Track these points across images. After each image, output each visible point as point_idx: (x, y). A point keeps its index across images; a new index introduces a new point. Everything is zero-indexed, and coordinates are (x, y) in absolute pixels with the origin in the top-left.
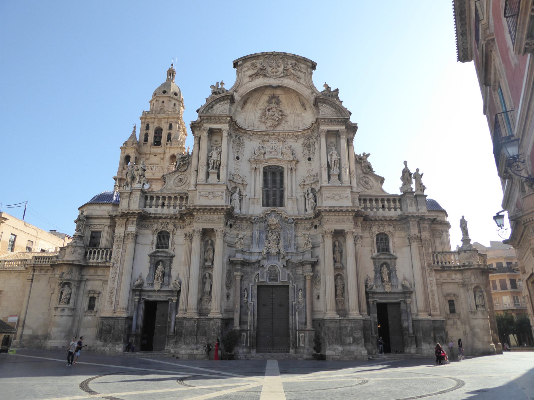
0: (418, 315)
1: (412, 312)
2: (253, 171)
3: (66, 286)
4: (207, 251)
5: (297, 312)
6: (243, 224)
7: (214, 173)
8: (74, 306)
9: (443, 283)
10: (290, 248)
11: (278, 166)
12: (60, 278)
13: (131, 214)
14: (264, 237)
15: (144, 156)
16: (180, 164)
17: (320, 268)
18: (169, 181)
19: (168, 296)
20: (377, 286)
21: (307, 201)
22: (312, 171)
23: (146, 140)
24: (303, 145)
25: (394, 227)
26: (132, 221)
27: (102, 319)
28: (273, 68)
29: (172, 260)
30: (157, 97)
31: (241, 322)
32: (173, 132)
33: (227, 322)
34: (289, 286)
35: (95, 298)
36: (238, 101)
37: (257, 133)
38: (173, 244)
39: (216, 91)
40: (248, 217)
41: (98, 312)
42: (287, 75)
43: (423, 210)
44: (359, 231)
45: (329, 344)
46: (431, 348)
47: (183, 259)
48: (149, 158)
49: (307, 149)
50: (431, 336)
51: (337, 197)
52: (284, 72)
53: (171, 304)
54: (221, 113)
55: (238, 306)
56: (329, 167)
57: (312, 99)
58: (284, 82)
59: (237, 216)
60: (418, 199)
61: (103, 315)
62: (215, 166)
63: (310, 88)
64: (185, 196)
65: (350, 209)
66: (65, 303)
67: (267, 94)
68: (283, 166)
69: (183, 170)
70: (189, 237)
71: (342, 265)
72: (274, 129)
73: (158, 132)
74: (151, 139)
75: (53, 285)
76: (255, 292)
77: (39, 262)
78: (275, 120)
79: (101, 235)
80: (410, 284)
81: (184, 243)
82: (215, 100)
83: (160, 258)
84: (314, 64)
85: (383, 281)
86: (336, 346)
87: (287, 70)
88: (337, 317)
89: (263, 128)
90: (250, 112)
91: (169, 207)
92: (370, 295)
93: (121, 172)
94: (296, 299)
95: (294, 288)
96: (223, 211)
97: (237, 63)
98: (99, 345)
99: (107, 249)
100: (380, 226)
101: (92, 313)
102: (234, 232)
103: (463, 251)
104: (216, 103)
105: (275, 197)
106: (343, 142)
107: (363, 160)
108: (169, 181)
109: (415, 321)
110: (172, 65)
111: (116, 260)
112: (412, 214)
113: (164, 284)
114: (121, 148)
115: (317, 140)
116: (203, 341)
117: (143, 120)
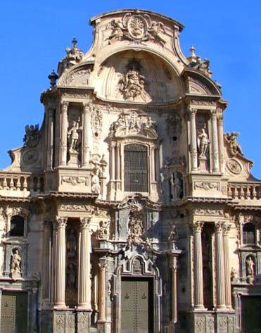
28: (136, 29)
44: (227, 223)
57: (180, 68)
81: (42, 229)
83: (15, 246)
85: (247, 274)
89: (120, 99)
91: (22, 189)
97: (95, 21)
115: (185, 118)
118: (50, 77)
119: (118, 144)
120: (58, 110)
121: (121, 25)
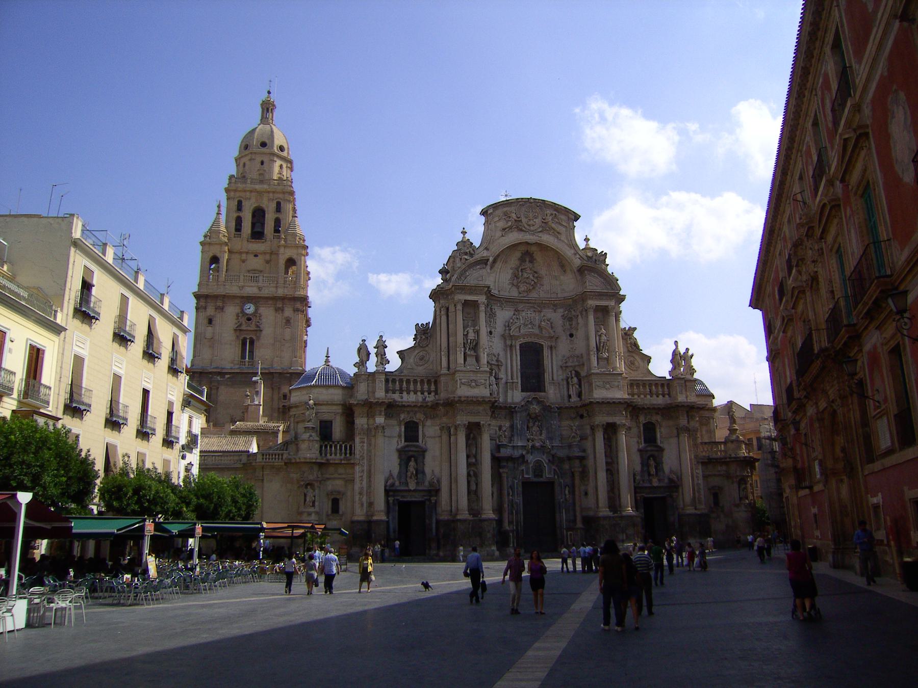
2: (508, 349)
3: (309, 487)
17: (590, 462)
19: (424, 496)
20: (643, 481)
21: (571, 387)
23: (238, 228)
30: (251, 153)
31: (510, 523)
33: (500, 522)
37: (509, 301)
38: (424, 436)
43: (692, 399)
48: (246, 260)
56: (598, 350)
57: (577, 262)
61: (356, 518)
62: (471, 346)
70: (448, 431)
71: (612, 459)
73: (259, 214)
76: (520, 489)
78: (530, 284)
80: (677, 478)
83: (411, 453)
87: (545, 223)
88: (611, 514)
89: (514, 293)
90: (500, 272)
91: (415, 393)
107: (629, 335)
110: (269, 92)
114: (202, 244)
115: (582, 314)
118: (440, 272)
119: (514, 342)
120: (452, 308)
121: (514, 216)
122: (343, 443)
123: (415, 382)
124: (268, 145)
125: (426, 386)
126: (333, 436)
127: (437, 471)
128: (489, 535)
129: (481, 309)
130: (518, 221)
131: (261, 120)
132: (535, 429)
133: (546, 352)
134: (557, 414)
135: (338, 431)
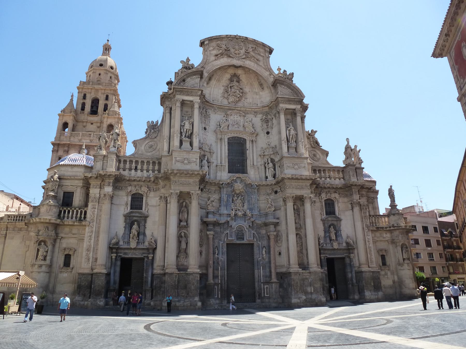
0: (360, 267)
1: (355, 265)
2: (219, 141)
3: (42, 243)
4: (182, 212)
5: (261, 267)
6: (211, 188)
7: (187, 141)
8: (50, 263)
9: (377, 241)
10: (254, 210)
11: (241, 138)
12: (36, 237)
13: (107, 176)
14: (231, 200)
15: (81, 124)
16: (151, 131)
17: (282, 227)
18: (140, 146)
19: (144, 253)
20: (326, 244)
21: (267, 169)
22: (271, 143)
23: (83, 109)
24: (262, 121)
25: (339, 194)
26: (108, 183)
27: (80, 275)
29: (146, 219)
31: (215, 277)
32: (109, 103)
33: (204, 276)
34: (254, 243)
35: (70, 255)
36: (206, 76)
37: (221, 108)
38: (147, 204)
39: (187, 66)
40: (217, 182)
41: (74, 270)
42: (248, 57)
45: (294, 294)
46: (372, 295)
47: (157, 219)
48: (86, 126)
49: (265, 124)
50: (371, 284)
51: (296, 167)
52: (246, 54)
53: (146, 261)
54: (192, 86)
55: (211, 262)
56: (288, 141)
57: (271, 79)
58: (246, 63)
59: (207, 180)
60: (357, 171)
61: (81, 271)
62: (187, 135)
63: (268, 70)
64: (157, 161)
65: (308, 178)
66: (42, 260)
67: (229, 73)
68: (245, 138)
69: (154, 137)
71: (300, 225)
72: (235, 104)
73: (95, 102)
74: (88, 108)
75: (28, 243)
76: (225, 249)
77: (12, 220)
79: (74, 196)
80: (353, 243)
81: (158, 205)
82: (187, 74)
83: (135, 218)
84: (272, 49)
86: (300, 295)
87: (248, 53)
89: (225, 102)
91: (142, 170)
92: (322, 251)
93: (59, 138)
94: (261, 255)
95: (259, 246)
96: (198, 176)
98: (79, 301)
99: (81, 208)
100: (328, 192)
101: (67, 269)
102: (205, 195)
103: (392, 214)
104: (188, 77)
105: (239, 165)
106: (299, 119)
107: (312, 136)
108: (140, 146)
109: (358, 272)
110: (108, 41)
111: (92, 219)
112: (355, 183)
113: (140, 242)
115: (275, 116)
116: (183, 294)
117: (81, 90)
119: (223, 136)
122: (79, 209)
123: (143, 162)
124: (104, 65)
125: (151, 167)
126: (73, 204)
127: (155, 234)
128: (193, 288)
129: (195, 107)
130: (227, 50)
131: (102, 54)
132: (239, 201)
133: (248, 145)
134: (256, 190)
135: (77, 200)
